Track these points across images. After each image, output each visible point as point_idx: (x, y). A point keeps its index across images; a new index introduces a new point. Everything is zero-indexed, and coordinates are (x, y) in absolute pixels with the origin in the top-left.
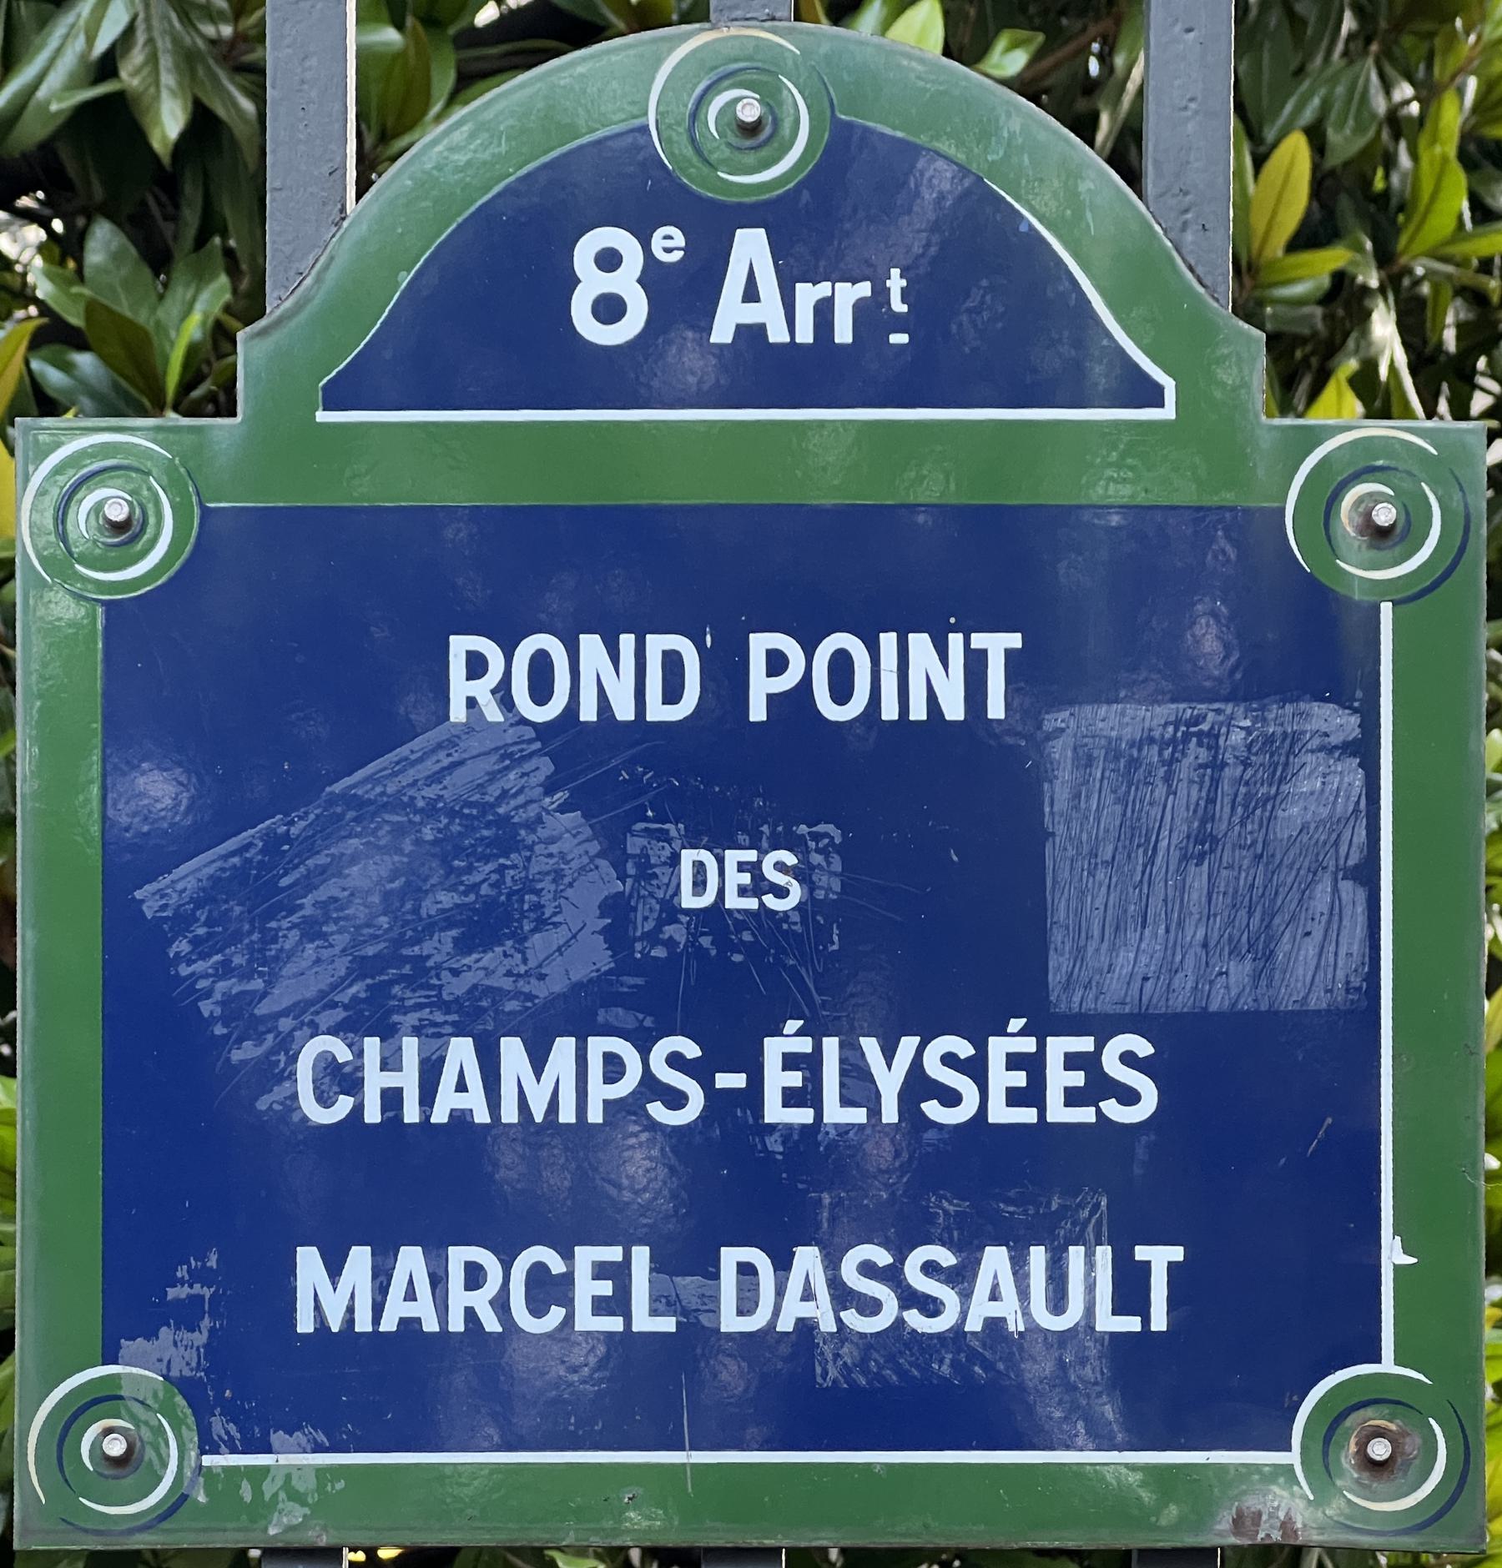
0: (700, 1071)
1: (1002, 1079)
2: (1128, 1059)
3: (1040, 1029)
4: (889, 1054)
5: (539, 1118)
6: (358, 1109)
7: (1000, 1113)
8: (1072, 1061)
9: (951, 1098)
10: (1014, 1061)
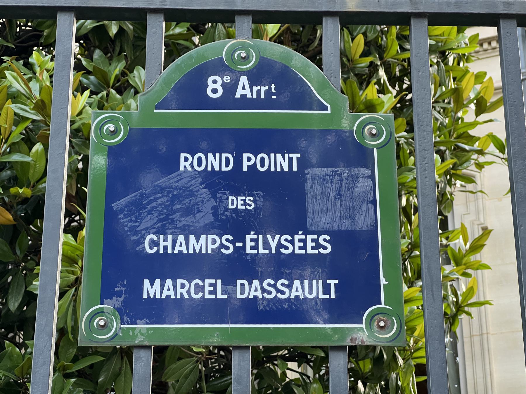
0: (233, 242)
1: (297, 244)
2: (325, 240)
3: (306, 234)
5: (197, 252)
6: (158, 250)
7: (297, 251)
8: (312, 240)
9: (287, 248)
10: (300, 240)
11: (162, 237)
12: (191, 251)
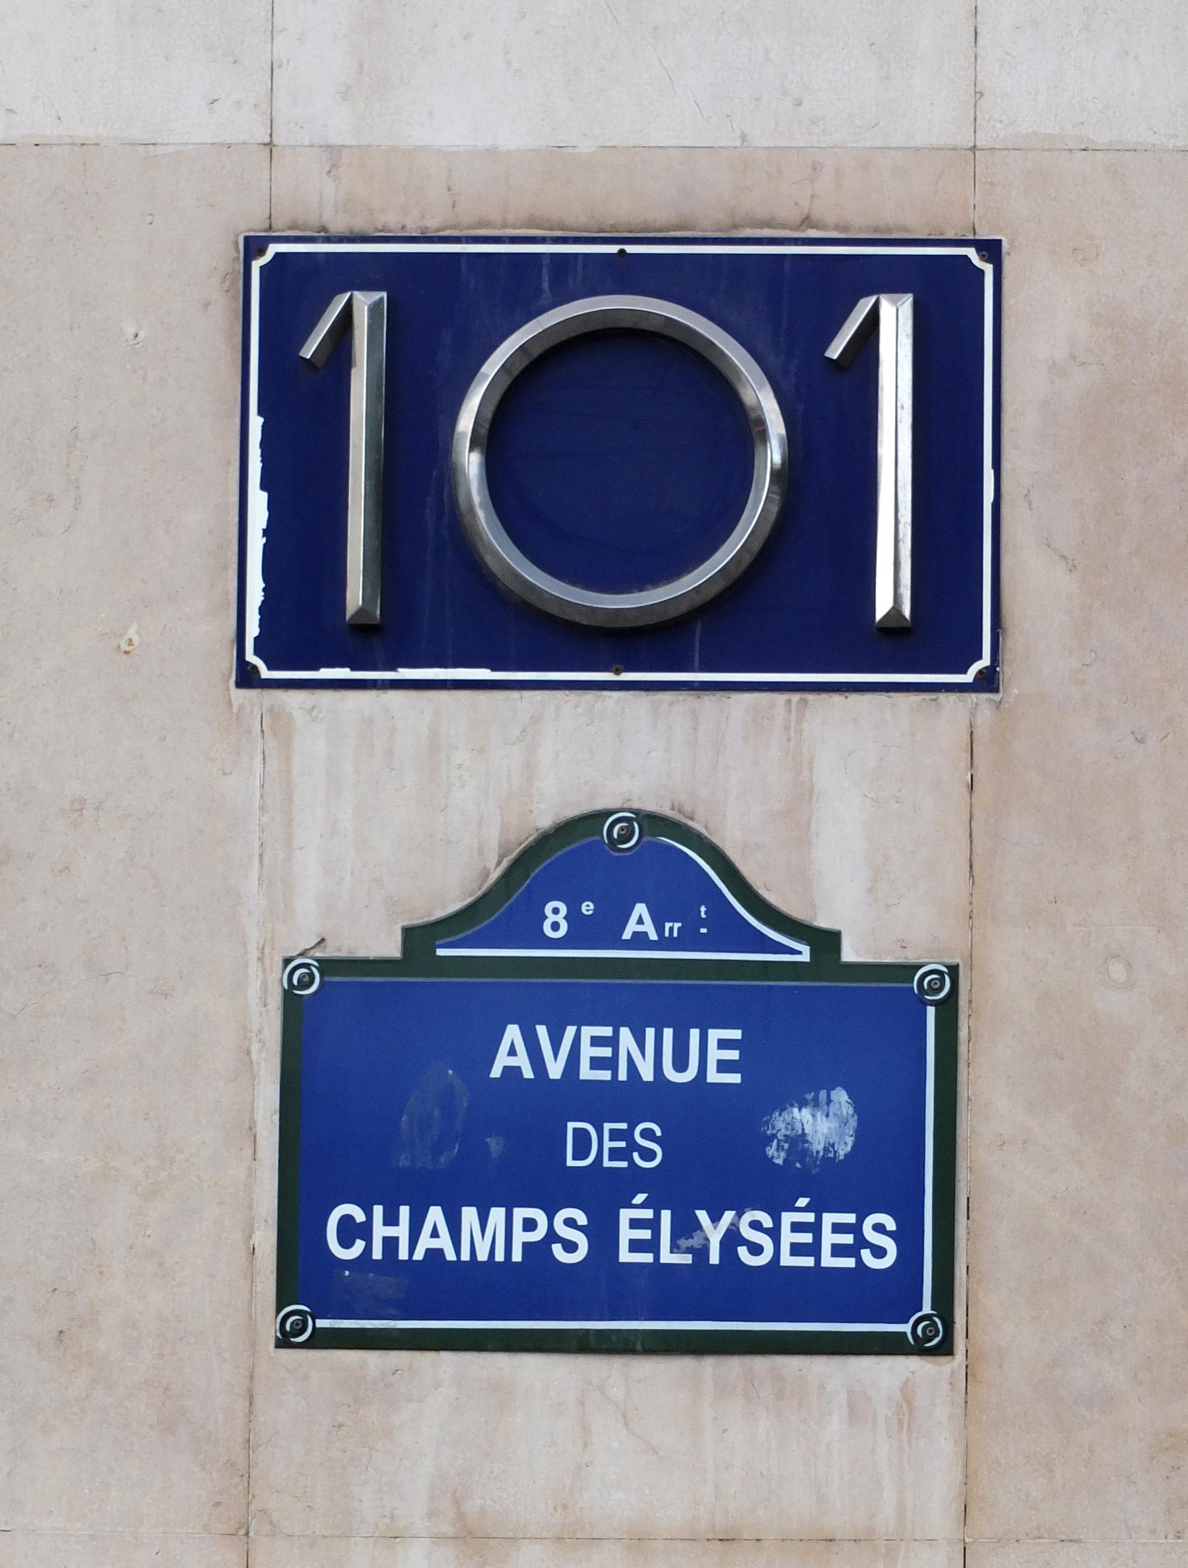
1: (788, 1237)
3: (819, 1207)
4: (715, 1219)
6: (368, 1249)
7: (787, 1260)
10: (797, 1227)
11: (378, 1210)
12: (465, 1256)
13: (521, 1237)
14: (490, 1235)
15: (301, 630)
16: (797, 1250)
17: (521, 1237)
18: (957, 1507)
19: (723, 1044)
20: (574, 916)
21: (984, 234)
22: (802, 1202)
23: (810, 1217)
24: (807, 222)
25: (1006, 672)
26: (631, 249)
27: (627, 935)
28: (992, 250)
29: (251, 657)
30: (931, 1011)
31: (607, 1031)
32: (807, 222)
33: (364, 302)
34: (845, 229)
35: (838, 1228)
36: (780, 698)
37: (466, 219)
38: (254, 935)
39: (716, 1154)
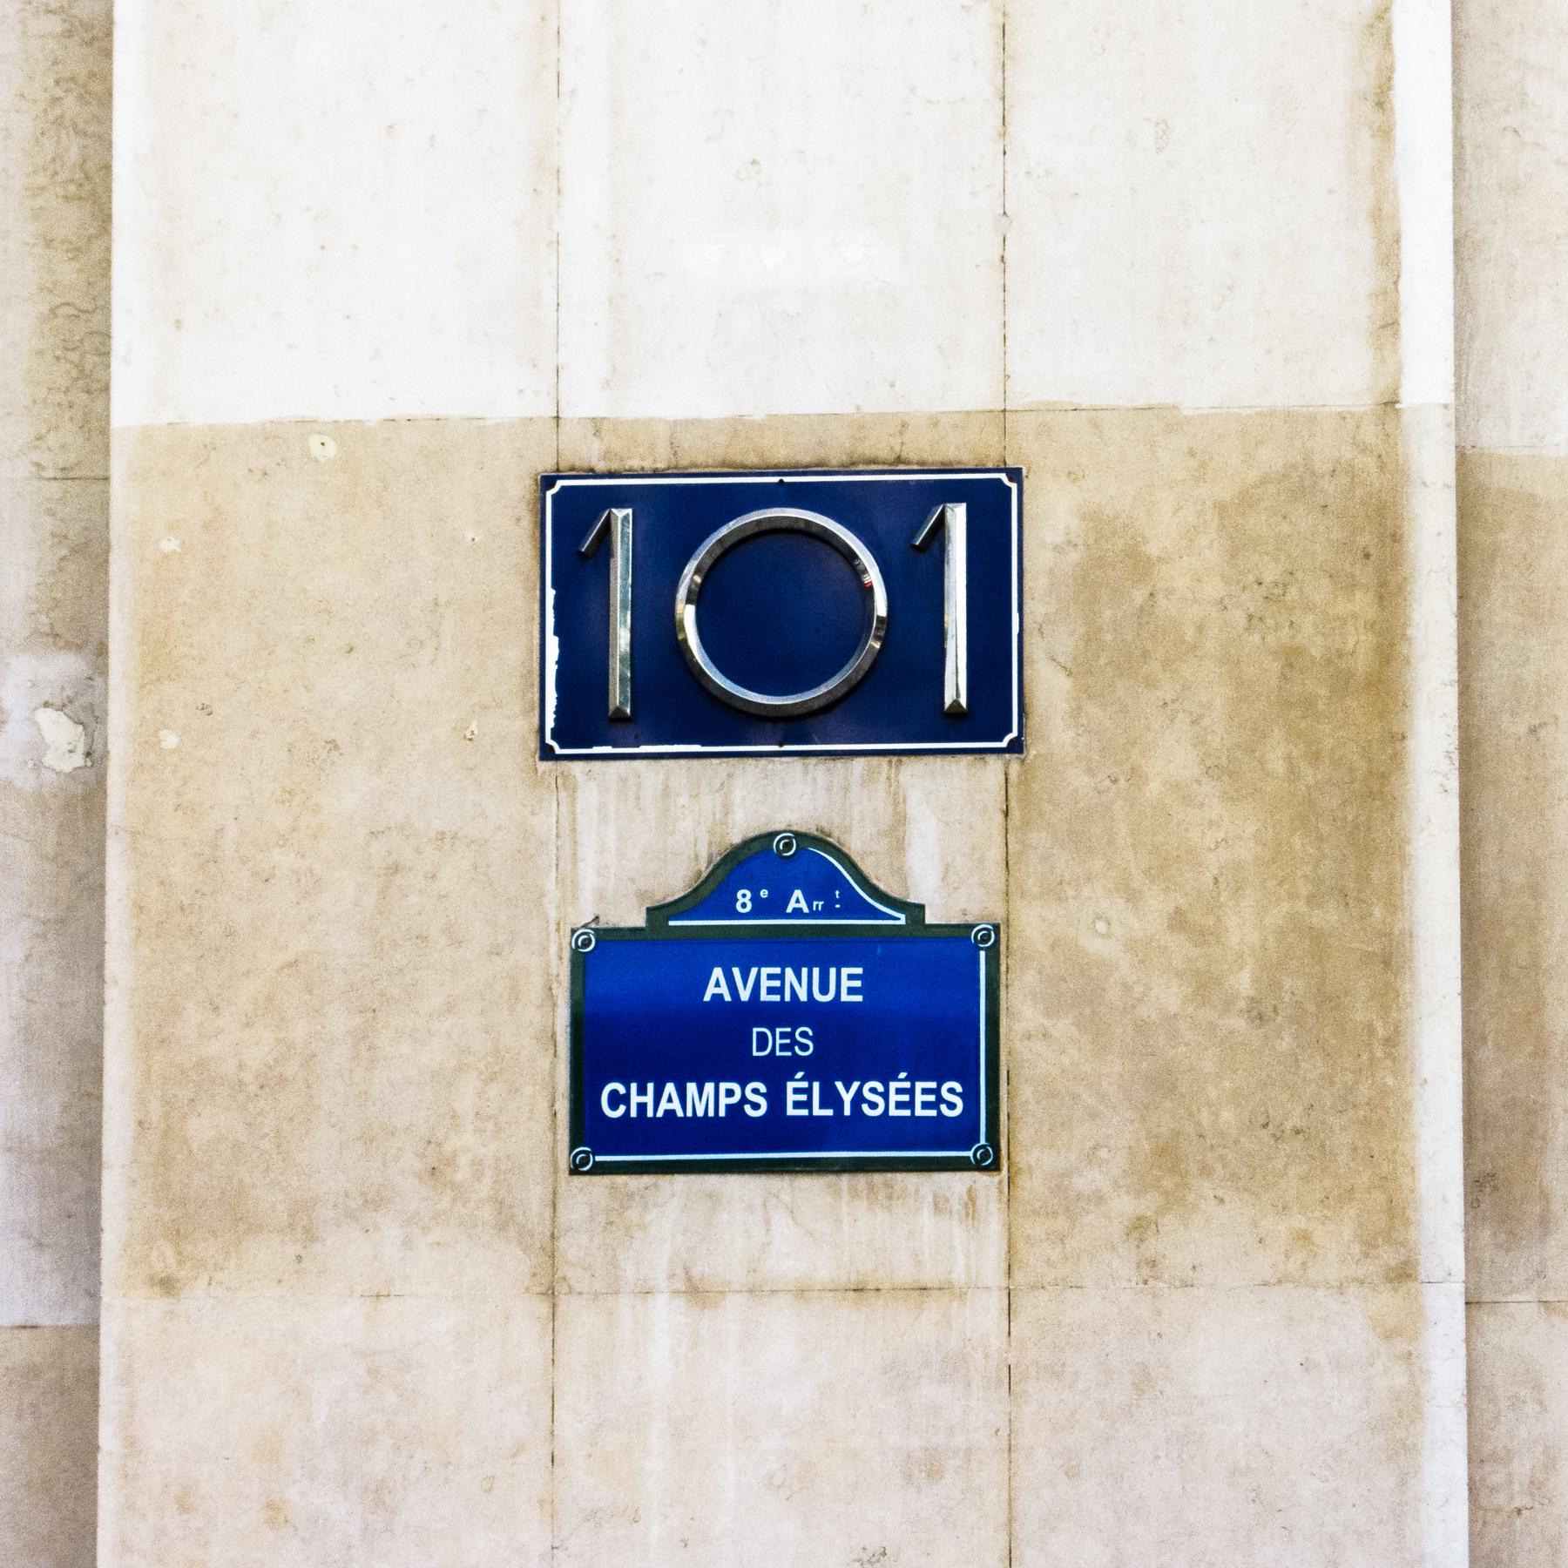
1: (893, 1098)
4: (847, 1090)
6: (628, 1110)
7: (893, 1112)
10: (899, 1091)
11: (634, 1086)
12: (689, 1114)
13: (724, 1101)
14: (705, 1099)
15: (582, 721)
16: (899, 1105)
17: (724, 1101)
18: (1004, 1266)
19: (851, 977)
20: (755, 899)
21: (1011, 464)
22: (903, 1075)
23: (907, 1085)
24: (899, 460)
25: (1028, 740)
26: (787, 479)
27: (789, 910)
28: (1016, 474)
29: (549, 740)
30: (982, 954)
31: (777, 970)
32: (899, 460)
33: (621, 514)
34: (923, 463)
35: (925, 1091)
36: (884, 760)
37: (684, 462)
38: (553, 915)
39: (846, 1045)
